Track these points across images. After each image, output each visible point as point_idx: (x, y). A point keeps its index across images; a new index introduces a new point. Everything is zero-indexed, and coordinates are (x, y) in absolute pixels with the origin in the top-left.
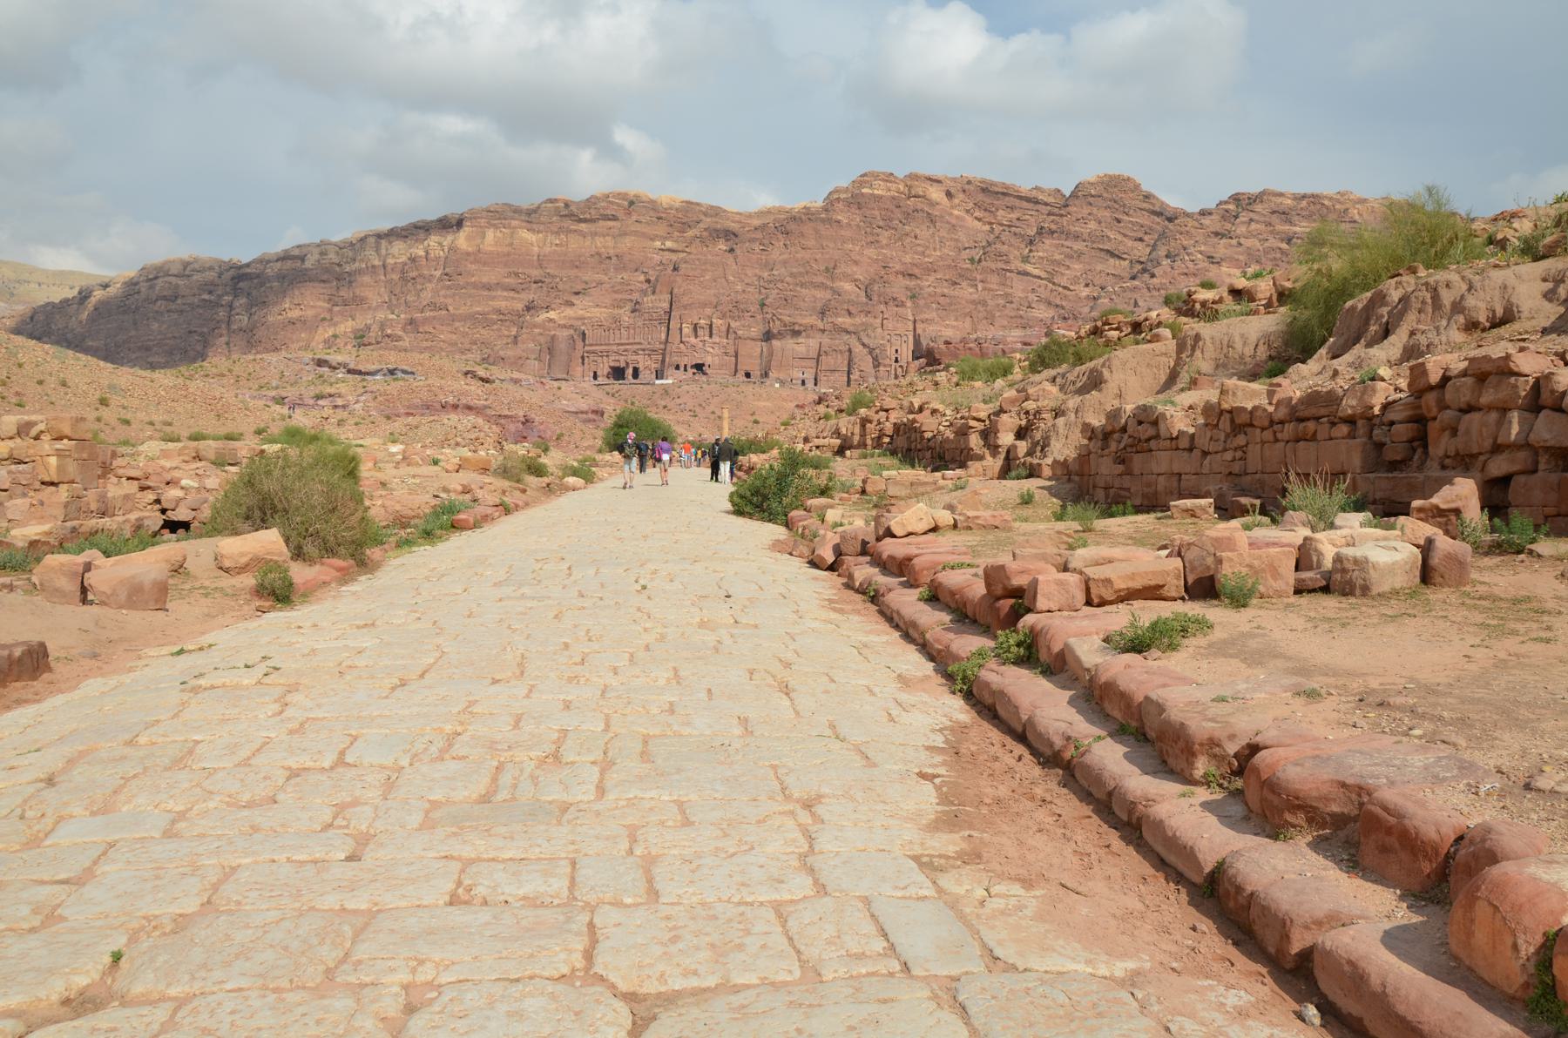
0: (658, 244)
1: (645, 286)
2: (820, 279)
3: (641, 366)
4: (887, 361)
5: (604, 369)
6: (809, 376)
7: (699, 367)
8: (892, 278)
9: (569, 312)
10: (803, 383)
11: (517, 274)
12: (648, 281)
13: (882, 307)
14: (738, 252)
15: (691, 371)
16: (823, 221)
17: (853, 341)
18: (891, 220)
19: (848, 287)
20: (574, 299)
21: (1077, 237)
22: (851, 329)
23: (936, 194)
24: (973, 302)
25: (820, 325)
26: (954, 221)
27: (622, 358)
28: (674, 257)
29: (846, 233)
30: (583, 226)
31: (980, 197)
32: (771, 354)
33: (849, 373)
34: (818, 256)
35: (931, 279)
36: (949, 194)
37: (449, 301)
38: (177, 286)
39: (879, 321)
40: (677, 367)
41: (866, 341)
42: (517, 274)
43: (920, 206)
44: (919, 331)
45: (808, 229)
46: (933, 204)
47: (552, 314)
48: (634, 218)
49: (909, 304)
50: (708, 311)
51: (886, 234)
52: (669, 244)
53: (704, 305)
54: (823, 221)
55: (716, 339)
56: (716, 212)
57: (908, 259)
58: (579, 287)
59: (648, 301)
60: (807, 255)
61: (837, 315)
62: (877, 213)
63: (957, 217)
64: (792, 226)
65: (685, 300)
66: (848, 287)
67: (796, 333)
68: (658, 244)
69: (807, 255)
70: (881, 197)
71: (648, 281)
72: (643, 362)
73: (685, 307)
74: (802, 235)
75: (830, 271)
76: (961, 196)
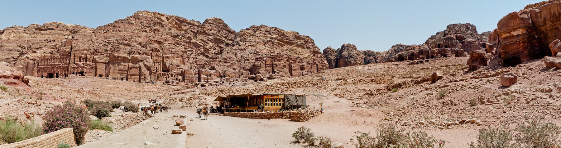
5: (46, 74)
6: (125, 76)
9: (34, 55)
11: (20, 46)
13: (151, 52)
15: (78, 74)
20: (36, 50)
24: (182, 51)
40: (73, 73)
41: (146, 63)
42: (20, 46)
43: (159, 21)
45: (121, 25)
47: (28, 56)
54: (127, 23)
55: (88, 62)
58: (38, 47)
60: (122, 34)
64: (116, 24)
65: (76, 48)
69: (122, 34)
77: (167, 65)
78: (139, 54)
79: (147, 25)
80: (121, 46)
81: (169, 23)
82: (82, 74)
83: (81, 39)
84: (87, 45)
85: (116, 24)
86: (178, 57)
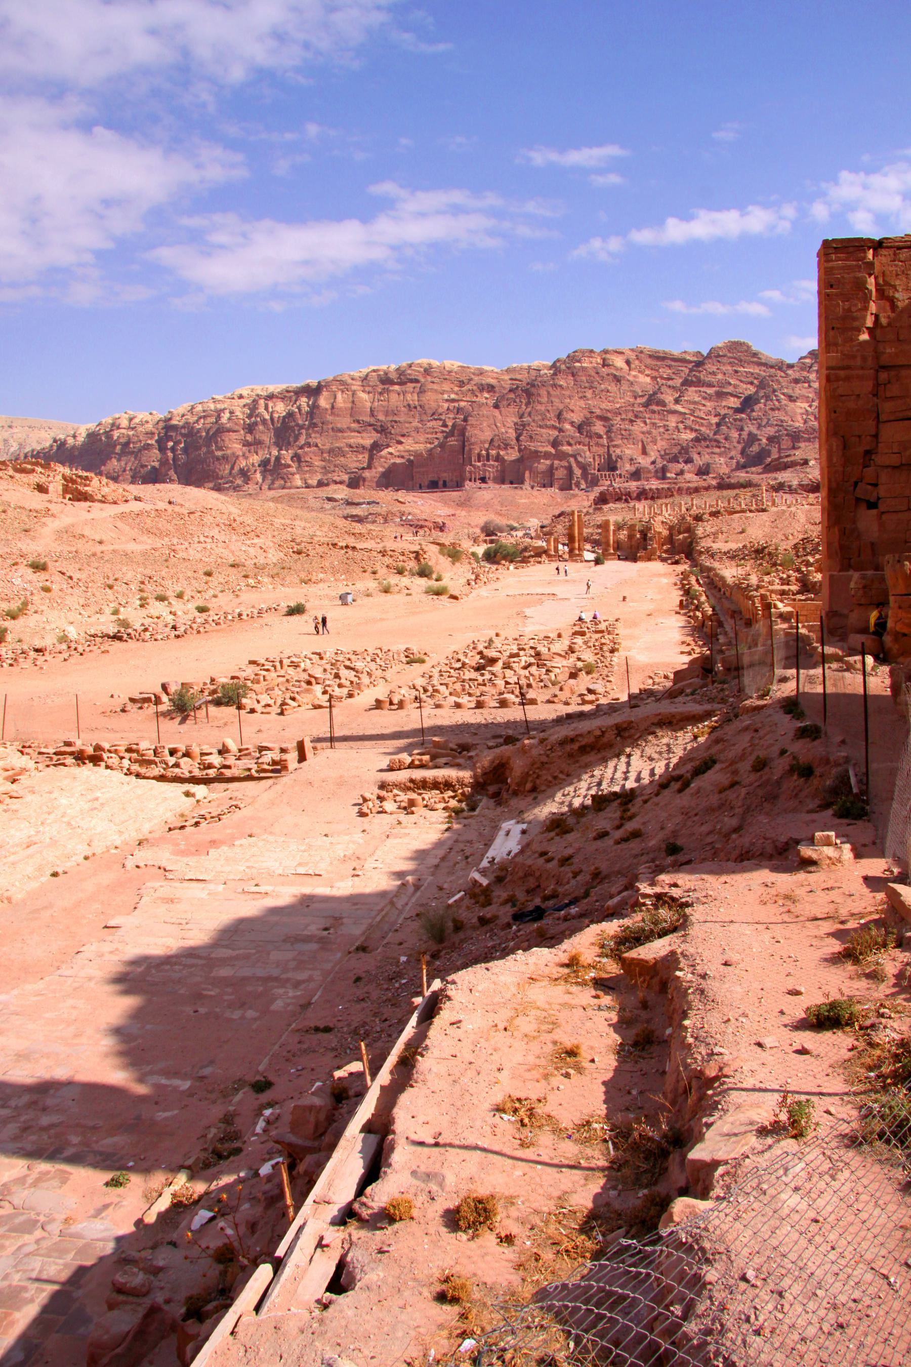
9: (400, 447)
12: (445, 425)
17: (572, 460)
19: (567, 426)
21: (710, 385)
23: (619, 362)
28: (456, 405)
29: (567, 393)
30: (396, 387)
31: (649, 361)
36: (628, 362)
37: (318, 441)
41: (580, 459)
47: (390, 450)
52: (453, 396)
53: (483, 442)
57: (603, 406)
58: (405, 431)
64: (533, 390)
66: (567, 426)
68: (446, 396)
75: (559, 416)
78: (570, 444)
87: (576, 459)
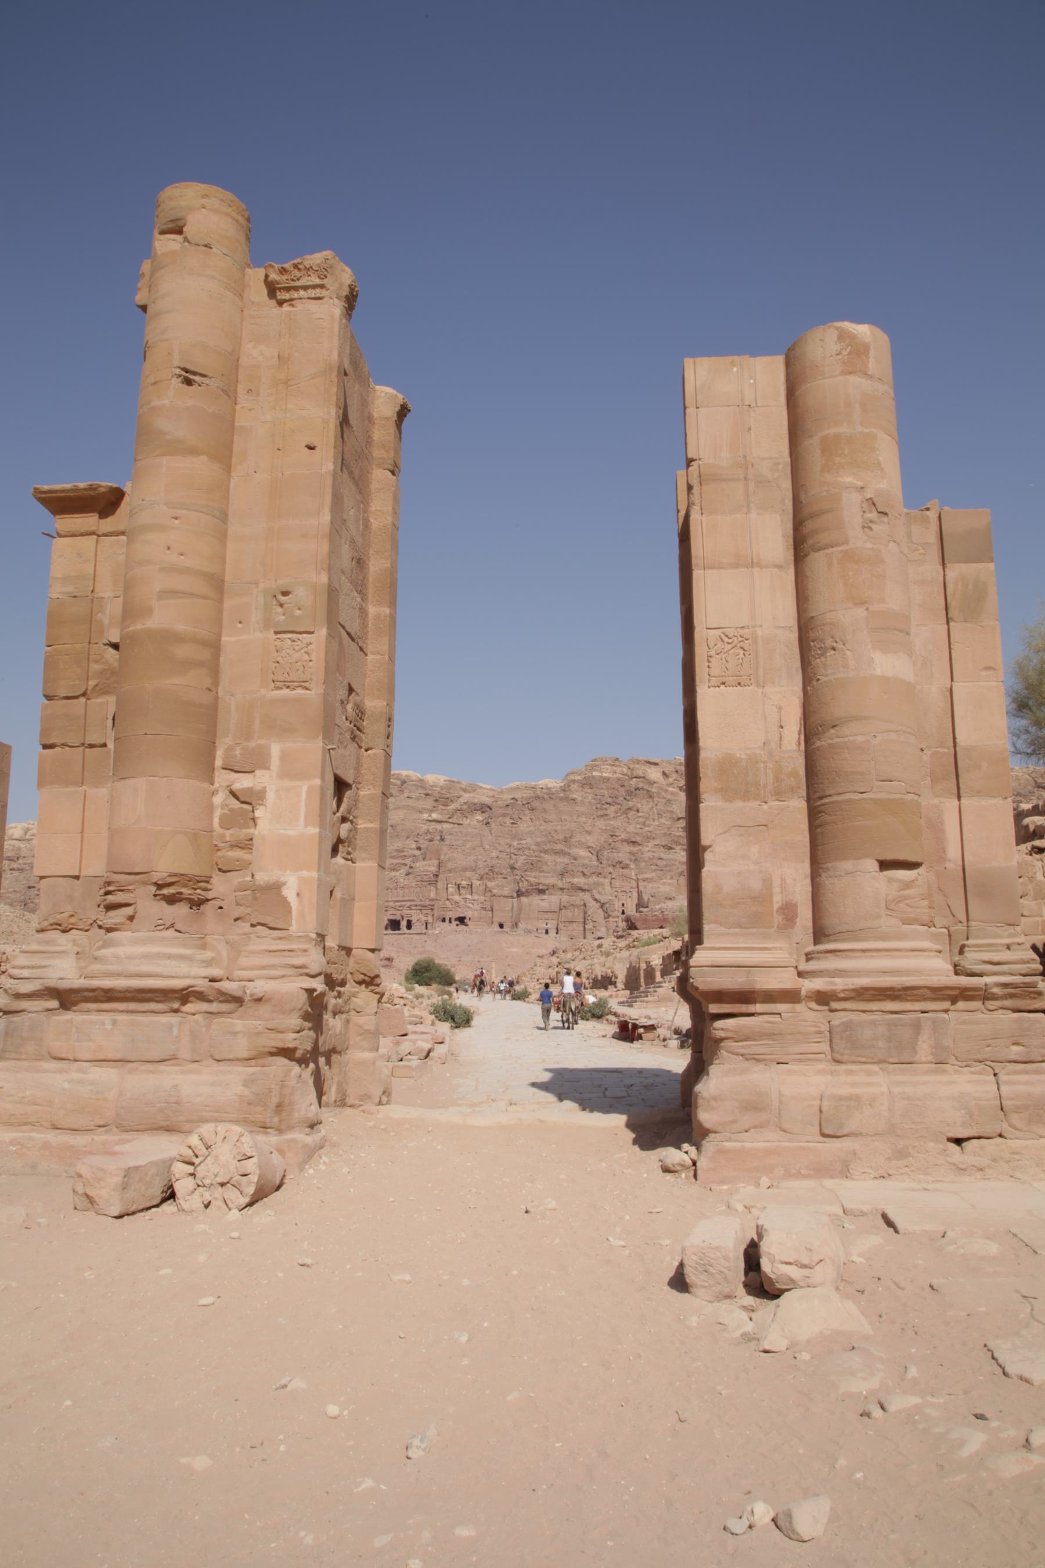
0: (425, 816)
1: (417, 853)
2: (559, 847)
3: (414, 919)
4: (616, 914)
7: (461, 920)
8: (618, 844)
10: (547, 932)
13: (611, 869)
14: (493, 826)
15: (454, 923)
16: (561, 799)
18: (617, 797)
19: (583, 853)
22: (586, 887)
23: (654, 774)
25: (560, 884)
26: (669, 797)
27: (398, 913)
28: (439, 827)
32: (520, 909)
33: (585, 923)
34: (559, 827)
35: (651, 844)
38: (19, 849)
39: (607, 881)
40: (444, 920)
41: (597, 897)
43: (640, 785)
44: (641, 888)
45: (549, 805)
46: (652, 783)
48: (406, 794)
49: (632, 866)
50: (468, 874)
51: (613, 808)
52: (435, 816)
53: (465, 869)
54: (561, 799)
56: (473, 788)
57: (631, 829)
59: (421, 866)
61: (573, 876)
62: (605, 792)
63: (672, 793)
64: (536, 804)
65: (450, 865)
67: (542, 892)
68: (425, 816)
70: (608, 779)
71: (419, 848)
72: (415, 916)
73: (450, 871)
74: (545, 810)
76: (675, 776)
77: (645, 897)
79: (609, 800)
80: (547, 857)
81: (671, 784)
82: (461, 920)
83: (459, 843)
84: (472, 858)
85: (536, 804)
86: (672, 878)
87: (592, 896)
